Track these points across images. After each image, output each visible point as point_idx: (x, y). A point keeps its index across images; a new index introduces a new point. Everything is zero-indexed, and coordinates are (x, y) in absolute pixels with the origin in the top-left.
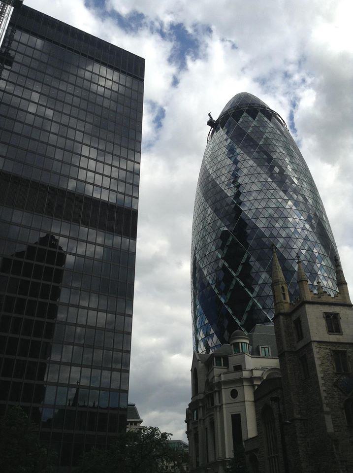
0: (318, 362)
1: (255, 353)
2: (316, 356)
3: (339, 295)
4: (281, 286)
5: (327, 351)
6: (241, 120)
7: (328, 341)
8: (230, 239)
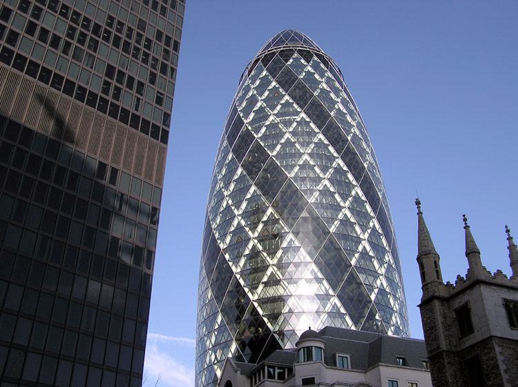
0: (502, 367)
1: (331, 362)
2: (500, 358)
3: (516, 277)
4: (433, 260)
5: (512, 352)
6: (291, 60)
7: (511, 338)
8: (268, 213)
